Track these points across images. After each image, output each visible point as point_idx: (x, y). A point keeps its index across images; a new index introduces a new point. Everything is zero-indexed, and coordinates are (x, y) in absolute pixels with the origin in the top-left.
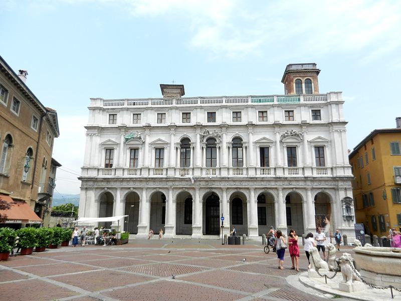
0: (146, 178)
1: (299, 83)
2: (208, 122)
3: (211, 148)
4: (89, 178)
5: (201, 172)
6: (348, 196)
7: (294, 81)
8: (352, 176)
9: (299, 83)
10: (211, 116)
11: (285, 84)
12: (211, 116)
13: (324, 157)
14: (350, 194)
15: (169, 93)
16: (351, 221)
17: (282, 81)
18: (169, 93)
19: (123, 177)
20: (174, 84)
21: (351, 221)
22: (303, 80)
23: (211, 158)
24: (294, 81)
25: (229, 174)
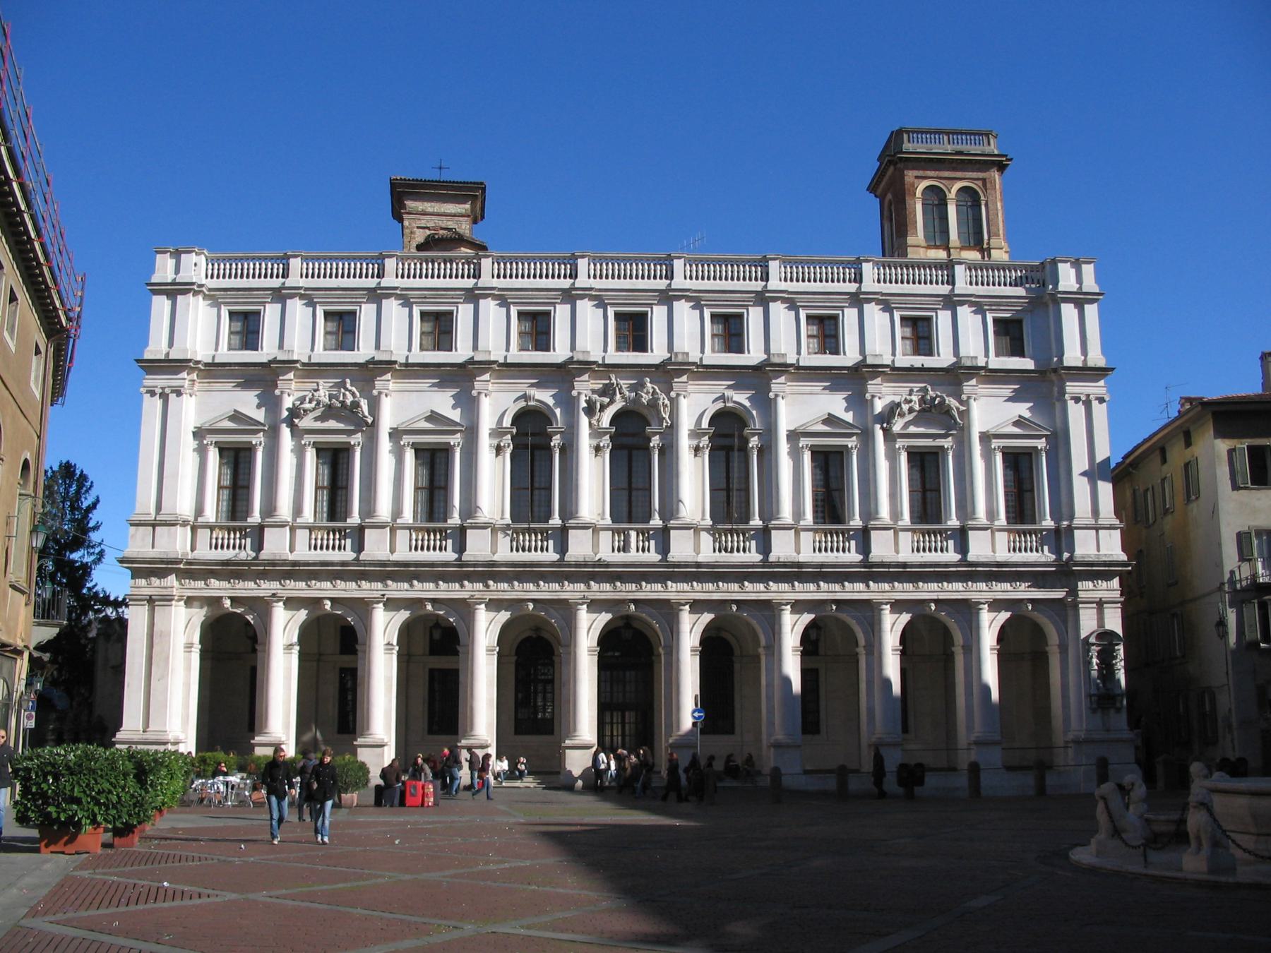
0: (383, 564)
1: (937, 200)
2: (618, 349)
3: (630, 449)
4: (162, 562)
5: (596, 545)
6: (1107, 627)
7: (919, 193)
8: (1123, 557)
9: (937, 200)
10: (633, 330)
11: (882, 199)
12: (633, 330)
13: (1032, 490)
14: (1114, 622)
15: (424, 213)
16: (1112, 711)
17: (872, 188)
18: (424, 213)
19: (291, 557)
20: (446, 176)
21: (1112, 711)
22: (952, 195)
23: (630, 489)
24: (919, 193)
25: (697, 550)
